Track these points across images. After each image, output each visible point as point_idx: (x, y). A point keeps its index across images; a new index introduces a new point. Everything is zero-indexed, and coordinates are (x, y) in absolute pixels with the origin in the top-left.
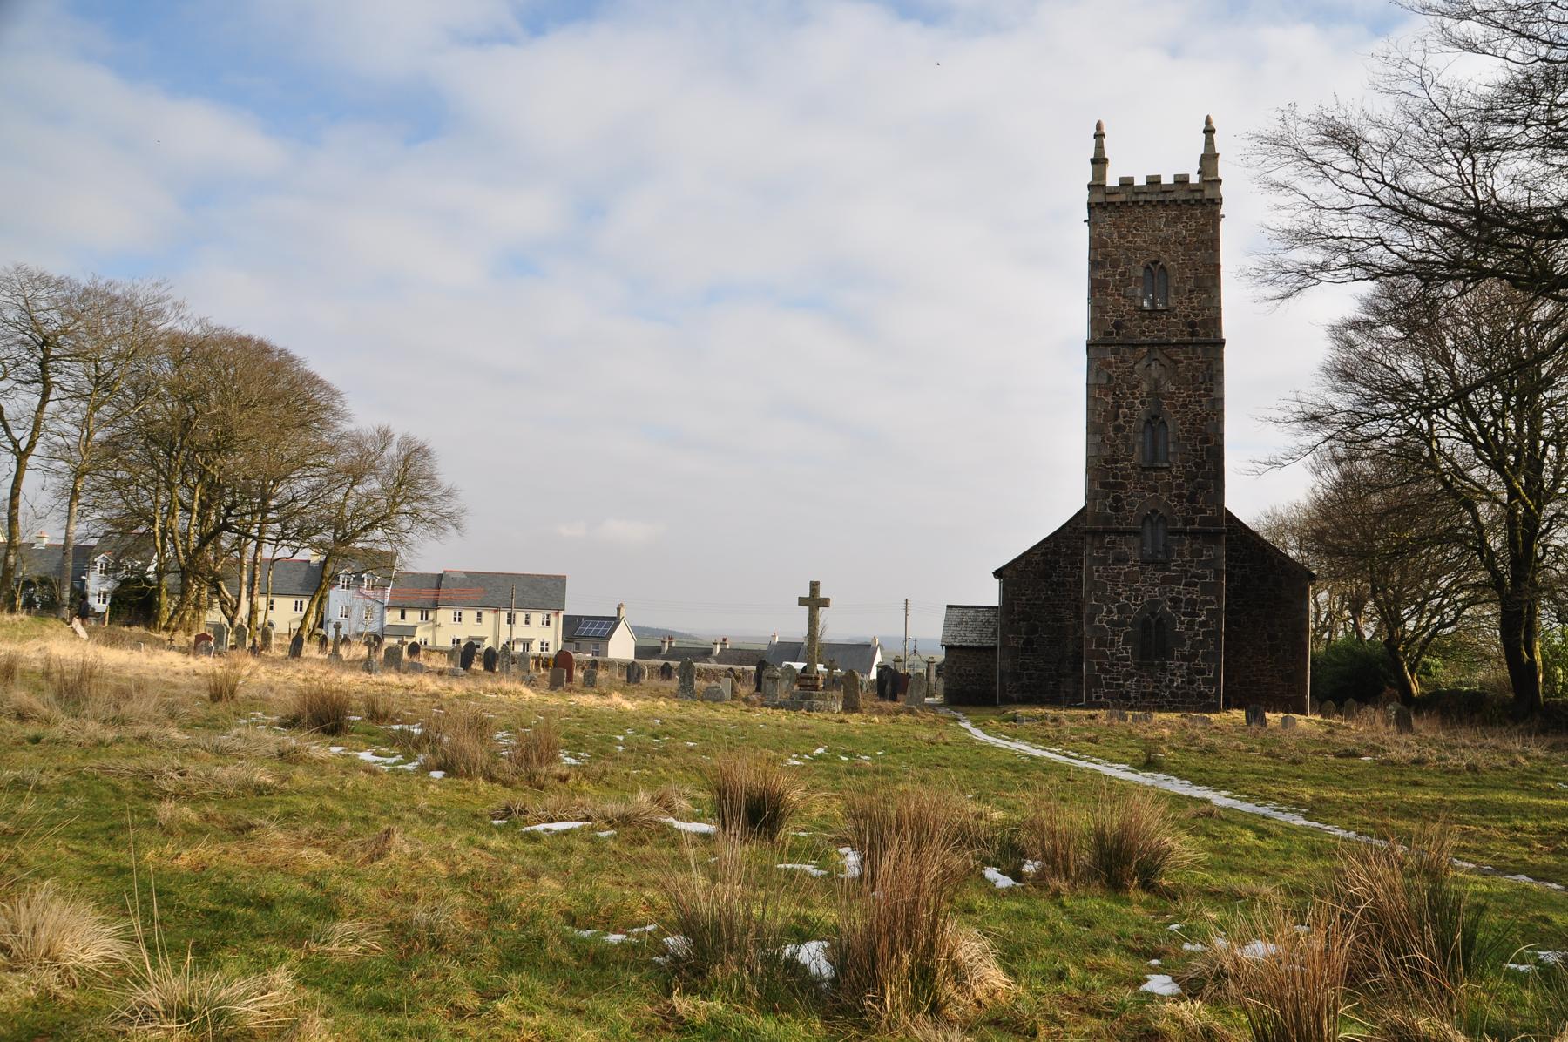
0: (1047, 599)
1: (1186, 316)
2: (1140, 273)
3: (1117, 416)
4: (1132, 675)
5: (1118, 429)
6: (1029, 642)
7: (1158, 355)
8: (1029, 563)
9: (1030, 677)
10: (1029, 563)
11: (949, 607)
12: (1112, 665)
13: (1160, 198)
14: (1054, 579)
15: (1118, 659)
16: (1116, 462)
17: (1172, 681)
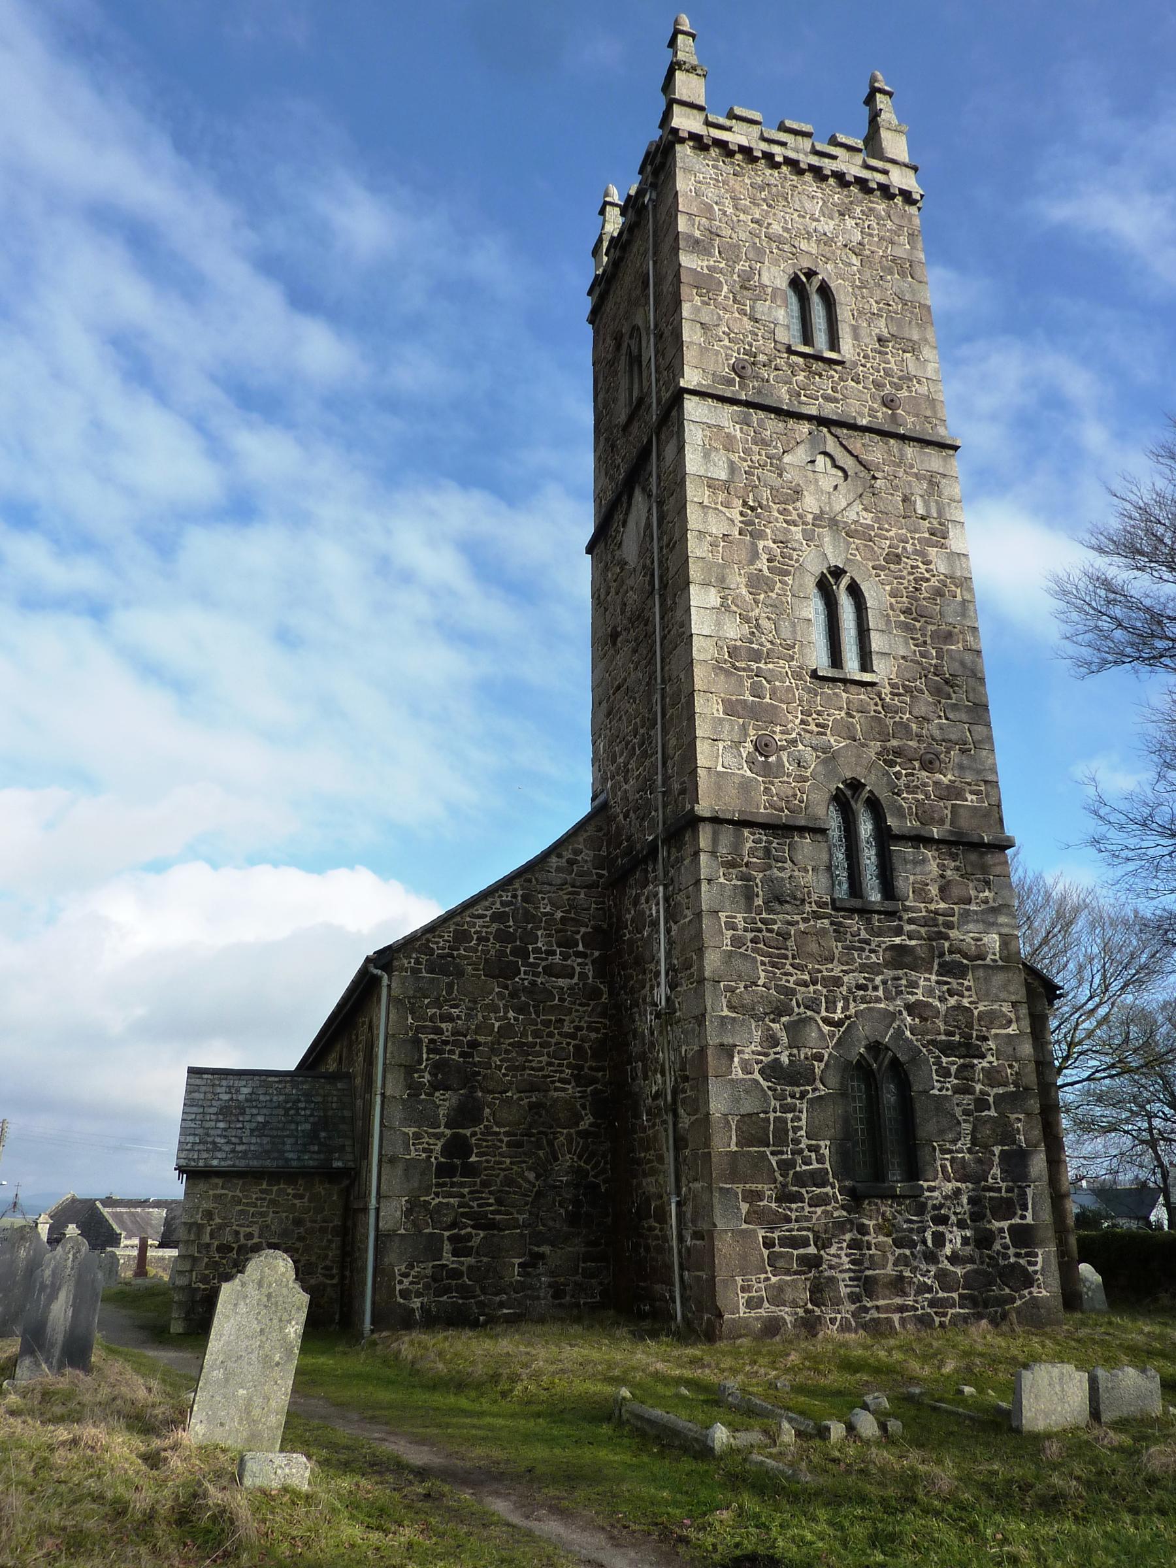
0: (507, 1030)
1: (878, 385)
2: (783, 283)
3: (754, 556)
4: (841, 1226)
5: (756, 583)
6: (457, 1147)
7: (831, 445)
8: (461, 937)
9: (460, 1247)
10: (461, 937)
11: (193, 1072)
12: (785, 1197)
13: (814, 160)
14: (523, 978)
15: (800, 1179)
16: (756, 656)
17: (939, 1240)
